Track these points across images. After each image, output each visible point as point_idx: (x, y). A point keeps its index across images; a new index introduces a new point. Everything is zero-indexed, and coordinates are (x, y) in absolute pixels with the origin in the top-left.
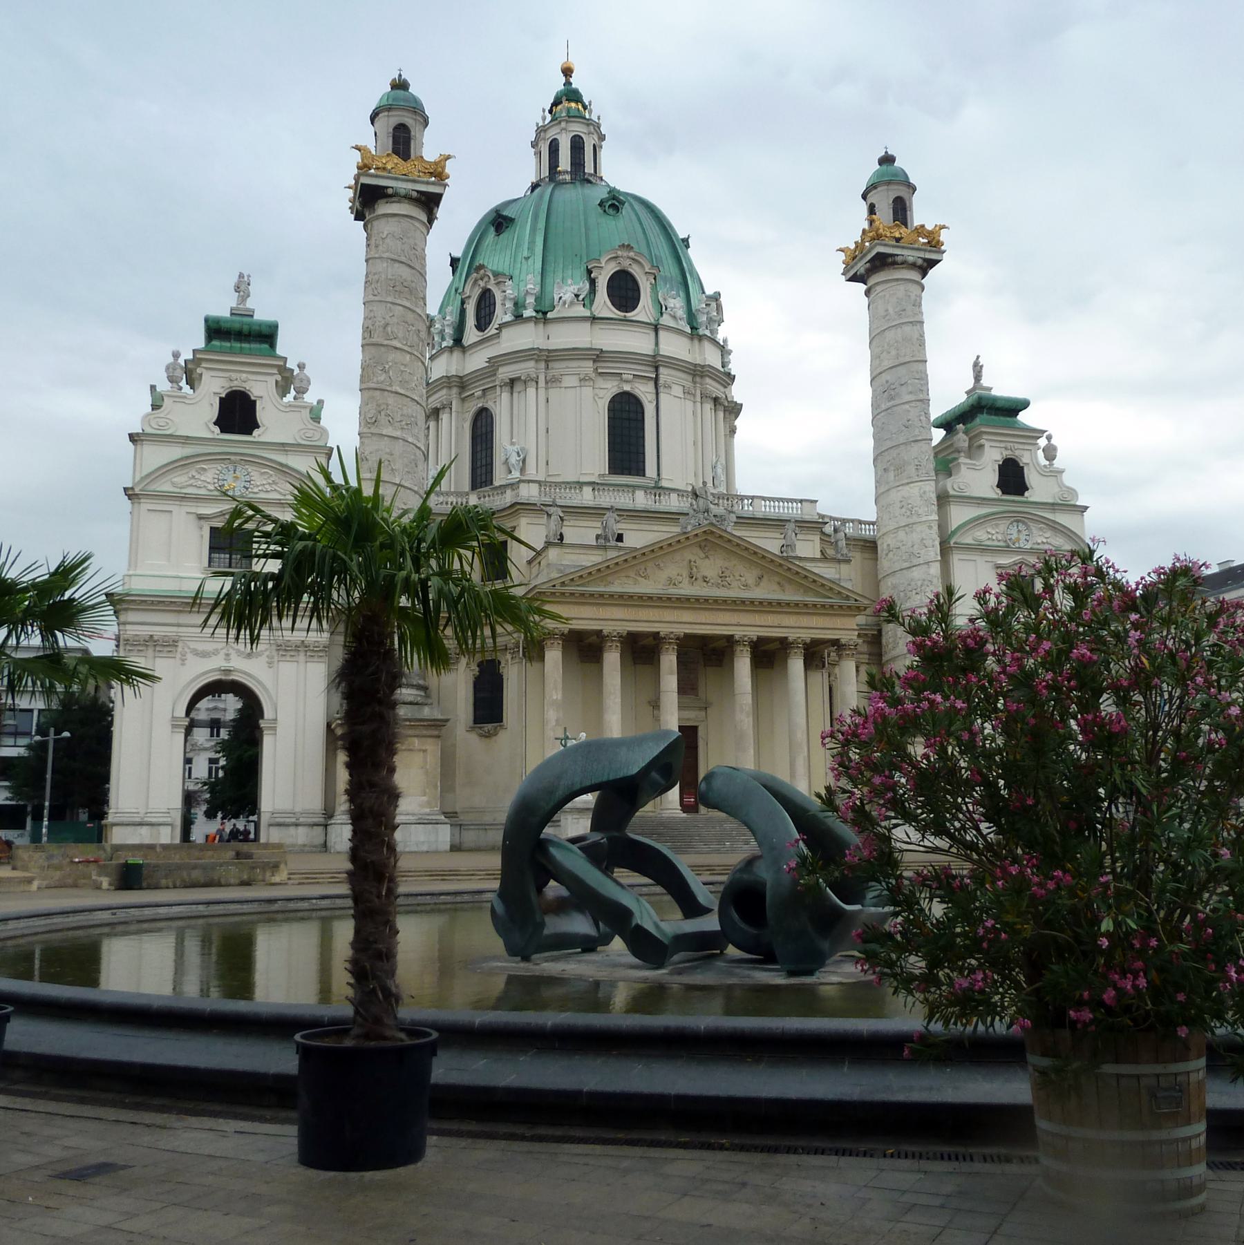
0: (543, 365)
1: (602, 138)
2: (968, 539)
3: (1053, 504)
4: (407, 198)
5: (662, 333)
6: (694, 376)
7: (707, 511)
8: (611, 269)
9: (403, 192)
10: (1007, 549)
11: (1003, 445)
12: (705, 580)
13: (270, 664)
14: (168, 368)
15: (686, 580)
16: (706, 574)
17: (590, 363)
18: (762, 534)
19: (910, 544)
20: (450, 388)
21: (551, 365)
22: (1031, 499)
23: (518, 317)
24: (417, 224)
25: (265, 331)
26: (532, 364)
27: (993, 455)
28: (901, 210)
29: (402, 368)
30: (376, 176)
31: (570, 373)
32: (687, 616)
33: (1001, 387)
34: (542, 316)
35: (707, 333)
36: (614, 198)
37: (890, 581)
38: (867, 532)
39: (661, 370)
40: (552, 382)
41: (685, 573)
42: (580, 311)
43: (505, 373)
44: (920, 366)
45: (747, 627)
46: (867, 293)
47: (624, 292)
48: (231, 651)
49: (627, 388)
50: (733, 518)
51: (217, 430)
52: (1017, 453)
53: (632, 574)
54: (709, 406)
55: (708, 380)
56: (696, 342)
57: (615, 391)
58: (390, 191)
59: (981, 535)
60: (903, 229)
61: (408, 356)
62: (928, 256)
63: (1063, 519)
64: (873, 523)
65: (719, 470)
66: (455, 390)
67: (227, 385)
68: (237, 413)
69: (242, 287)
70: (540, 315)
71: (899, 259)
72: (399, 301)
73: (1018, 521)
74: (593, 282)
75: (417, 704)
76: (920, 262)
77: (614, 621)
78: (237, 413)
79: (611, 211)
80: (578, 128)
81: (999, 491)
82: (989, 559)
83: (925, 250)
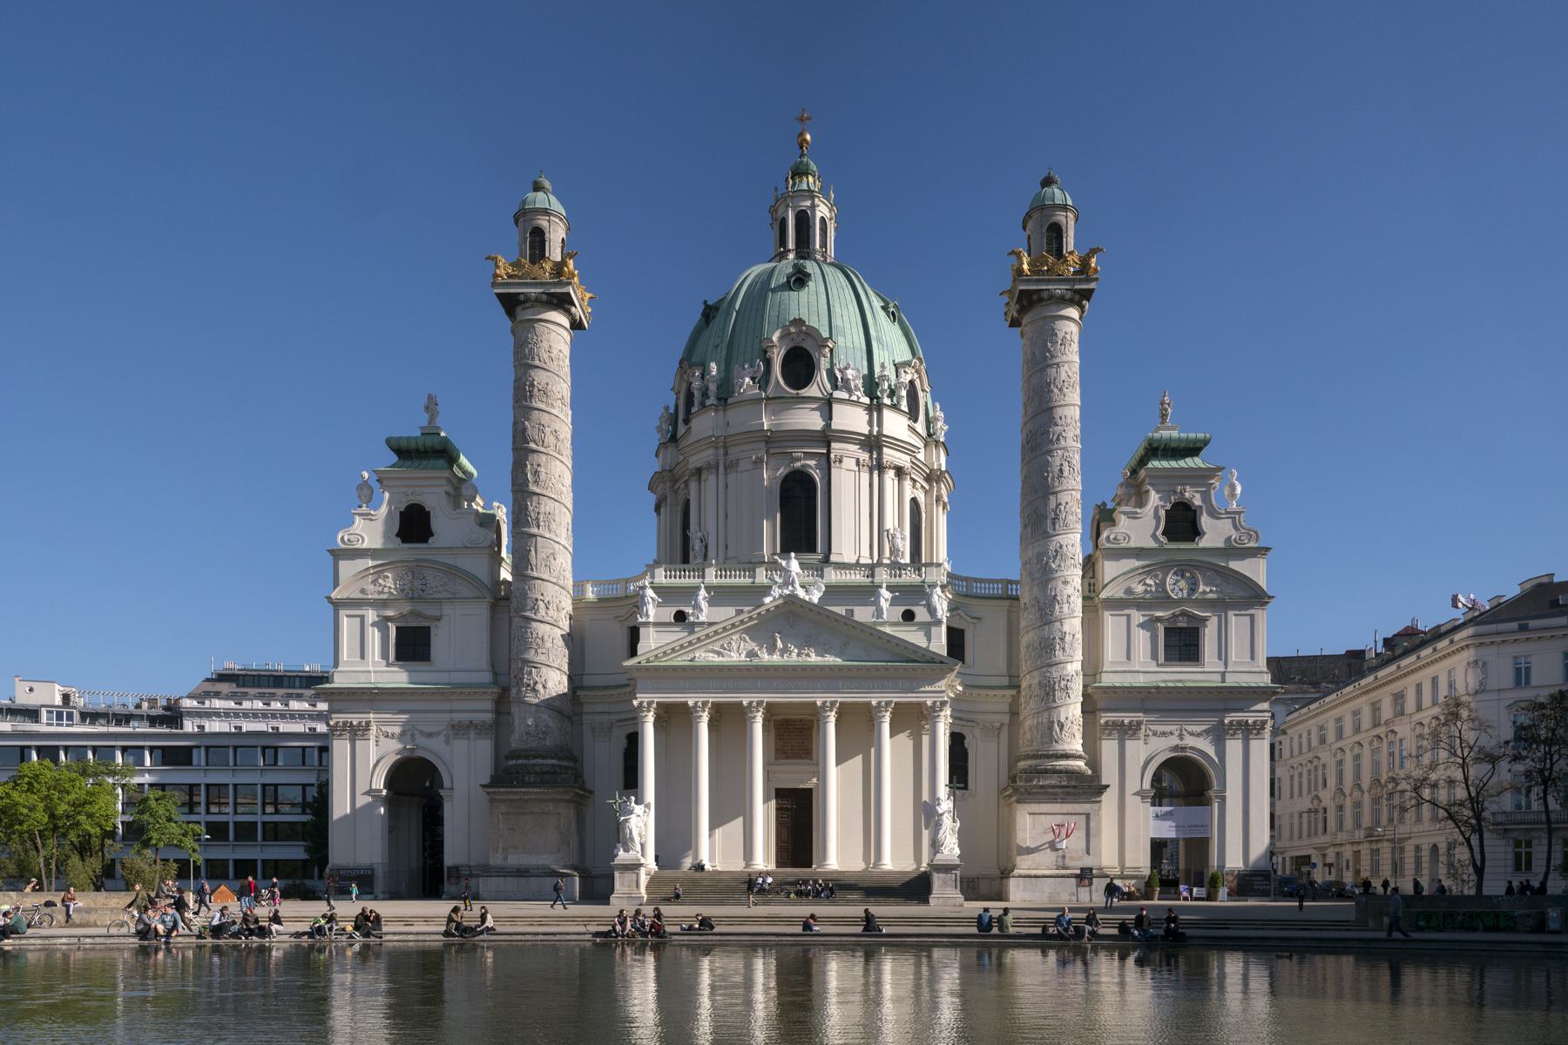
0: (721, 451)
5: (835, 407)
17: (763, 445)
21: (731, 451)
23: (703, 405)
26: (711, 451)
35: (887, 401)
39: (833, 445)
54: (891, 474)
63: (1235, 565)
64: (1017, 583)
74: (768, 363)
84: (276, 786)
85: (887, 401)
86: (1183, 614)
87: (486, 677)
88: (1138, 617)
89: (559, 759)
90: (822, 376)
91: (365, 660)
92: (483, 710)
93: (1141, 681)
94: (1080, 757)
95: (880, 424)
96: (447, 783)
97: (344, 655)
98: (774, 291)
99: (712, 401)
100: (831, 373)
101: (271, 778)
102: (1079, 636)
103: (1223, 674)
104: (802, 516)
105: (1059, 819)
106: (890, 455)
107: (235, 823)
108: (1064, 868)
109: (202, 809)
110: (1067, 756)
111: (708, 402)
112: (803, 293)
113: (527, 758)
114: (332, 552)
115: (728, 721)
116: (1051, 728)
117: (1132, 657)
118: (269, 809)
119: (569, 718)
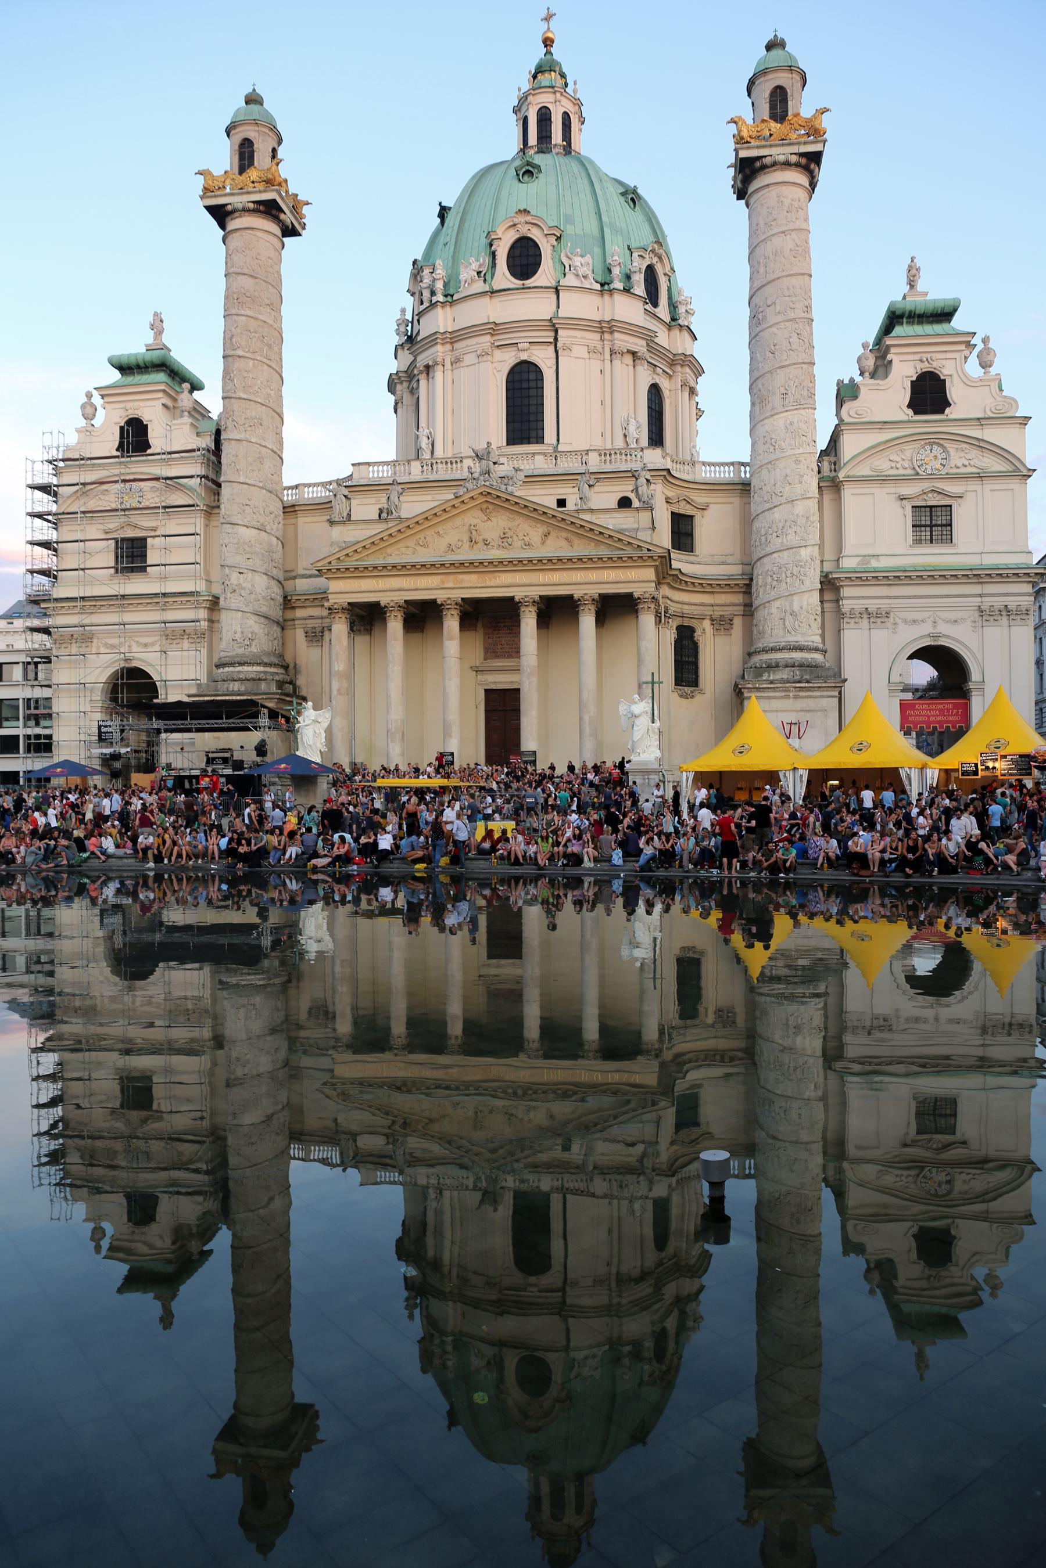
1: (578, 103)
2: (864, 471)
3: (978, 419)
4: (245, 210)
6: (603, 332)
7: (488, 472)
8: (511, 237)
9: (240, 206)
10: (916, 477)
11: (918, 357)
14: (83, 406)
15: (466, 545)
16: (486, 537)
17: (488, 338)
18: (543, 492)
19: (772, 482)
20: (401, 383)
21: (456, 346)
22: (951, 417)
24: (259, 234)
25: (156, 361)
27: (905, 369)
28: (779, 104)
29: (245, 374)
30: (215, 196)
33: (934, 291)
34: (451, 299)
36: (528, 164)
37: (756, 525)
38: (745, 474)
39: (560, 332)
40: (456, 361)
41: (466, 538)
42: (479, 286)
43: (423, 359)
44: (795, 281)
45: (526, 587)
46: (747, 205)
47: (524, 259)
48: (134, 644)
49: (524, 356)
50: (521, 476)
52: (935, 364)
53: (411, 543)
55: (616, 335)
56: (606, 297)
58: (229, 208)
59: (882, 464)
60: (774, 126)
61: (251, 363)
62: (804, 149)
63: (992, 434)
65: (632, 428)
66: (405, 384)
67: (124, 414)
68: (135, 437)
69: (157, 325)
70: (449, 299)
71: (767, 161)
72: (242, 312)
73: (931, 444)
74: (493, 255)
75: (260, 680)
76: (794, 159)
77: (391, 591)
78: (135, 437)
79: (526, 177)
80: (545, 99)
81: (910, 412)
82: (893, 490)
83: (799, 144)
85: (618, 285)
89: (266, 664)
94: (816, 650)
95: (613, 309)
99: (440, 298)
102: (816, 518)
105: (792, 717)
110: (800, 648)
111: (434, 299)
113: (232, 664)
116: (783, 619)
119: (278, 623)
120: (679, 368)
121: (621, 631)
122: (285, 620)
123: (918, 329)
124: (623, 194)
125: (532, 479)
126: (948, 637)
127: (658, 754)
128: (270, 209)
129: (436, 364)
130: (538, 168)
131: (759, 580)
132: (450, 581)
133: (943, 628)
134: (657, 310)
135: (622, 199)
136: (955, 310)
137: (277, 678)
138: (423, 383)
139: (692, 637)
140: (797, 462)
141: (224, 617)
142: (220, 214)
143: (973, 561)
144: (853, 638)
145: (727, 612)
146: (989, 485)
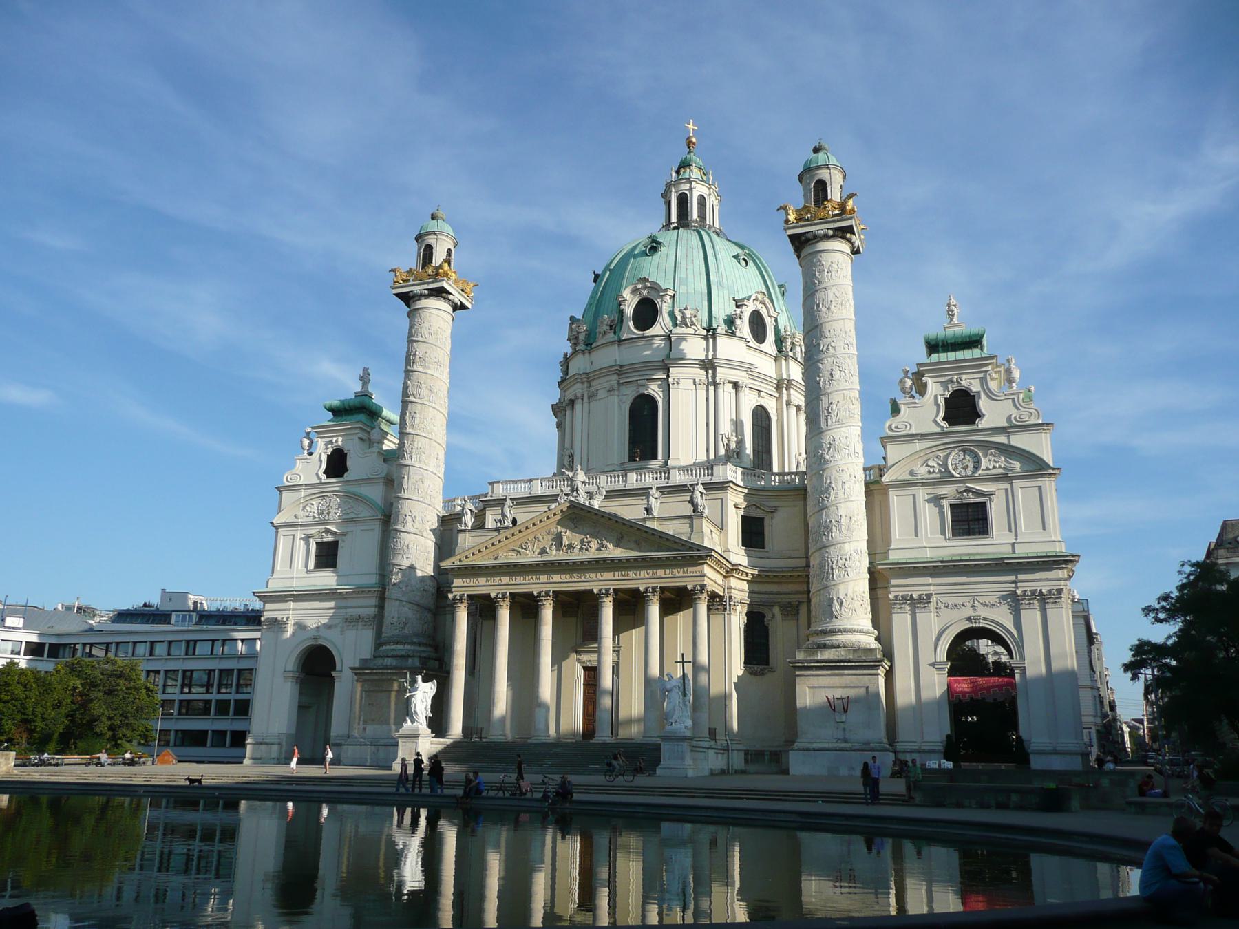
0: (586, 384)
12: (570, 546)
13: (342, 633)
17: (615, 377)
21: (593, 383)
22: (981, 426)
25: (358, 405)
26: (578, 386)
27: (936, 390)
31: (601, 384)
32: (557, 578)
36: (653, 241)
42: (611, 336)
43: (569, 395)
49: (643, 391)
51: (323, 477)
52: (963, 383)
54: (726, 392)
57: (634, 395)
61: (419, 407)
63: (1018, 440)
68: (337, 464)
71: (809, 236)
73: (964, 451)
76: (831, 233)
81: (944, 424)
82: (930, 491)
84: (192, 671)
86: (968, 490)
87: (373, 580)
88: (923, 494)
89: (412, 643)
90: (664, 320)
91: (295, 567)
92: (368, 607)
93: (928, 555)
96: (338, 667)
97: (278, 566)
98: (635, 256)
99: (581, 346)
100: (672, 315)
101: (190, 665)
103: (1013, 544)
104: (644, 432)
106: (722, 374)
107: (236, 701)
108: (845, 741)
109: (215, 689)
112: (656, 258)
114: (278, 488)
115: (526, 607)
116: (830, 606)
117: (921, 532)
118: (186, 690)
119: (429, 610)
120: (784, 391)
121: (681, 619)
122: (437, 607)
123: (951, 356)
124: (736, 257)
125: (611, 495)
126: (985, 619)
127: (689, 723)
128: (440, 293)
129: (577, 398)
130: (660, 243)
131: (812, 573)
132: (543, 578)
133: (983, 612)
134: (763, 347)
135: (734, 260)
136: (982, 336)
137: (423, 655)
138: (568, 412)
139: (763, 621)
140: (839, 471)
141: (388, 604)
142: (407, 298)
143: (1005, 551)
144: (901, 622)
145: (793, 599)
146: (1018, 484)
